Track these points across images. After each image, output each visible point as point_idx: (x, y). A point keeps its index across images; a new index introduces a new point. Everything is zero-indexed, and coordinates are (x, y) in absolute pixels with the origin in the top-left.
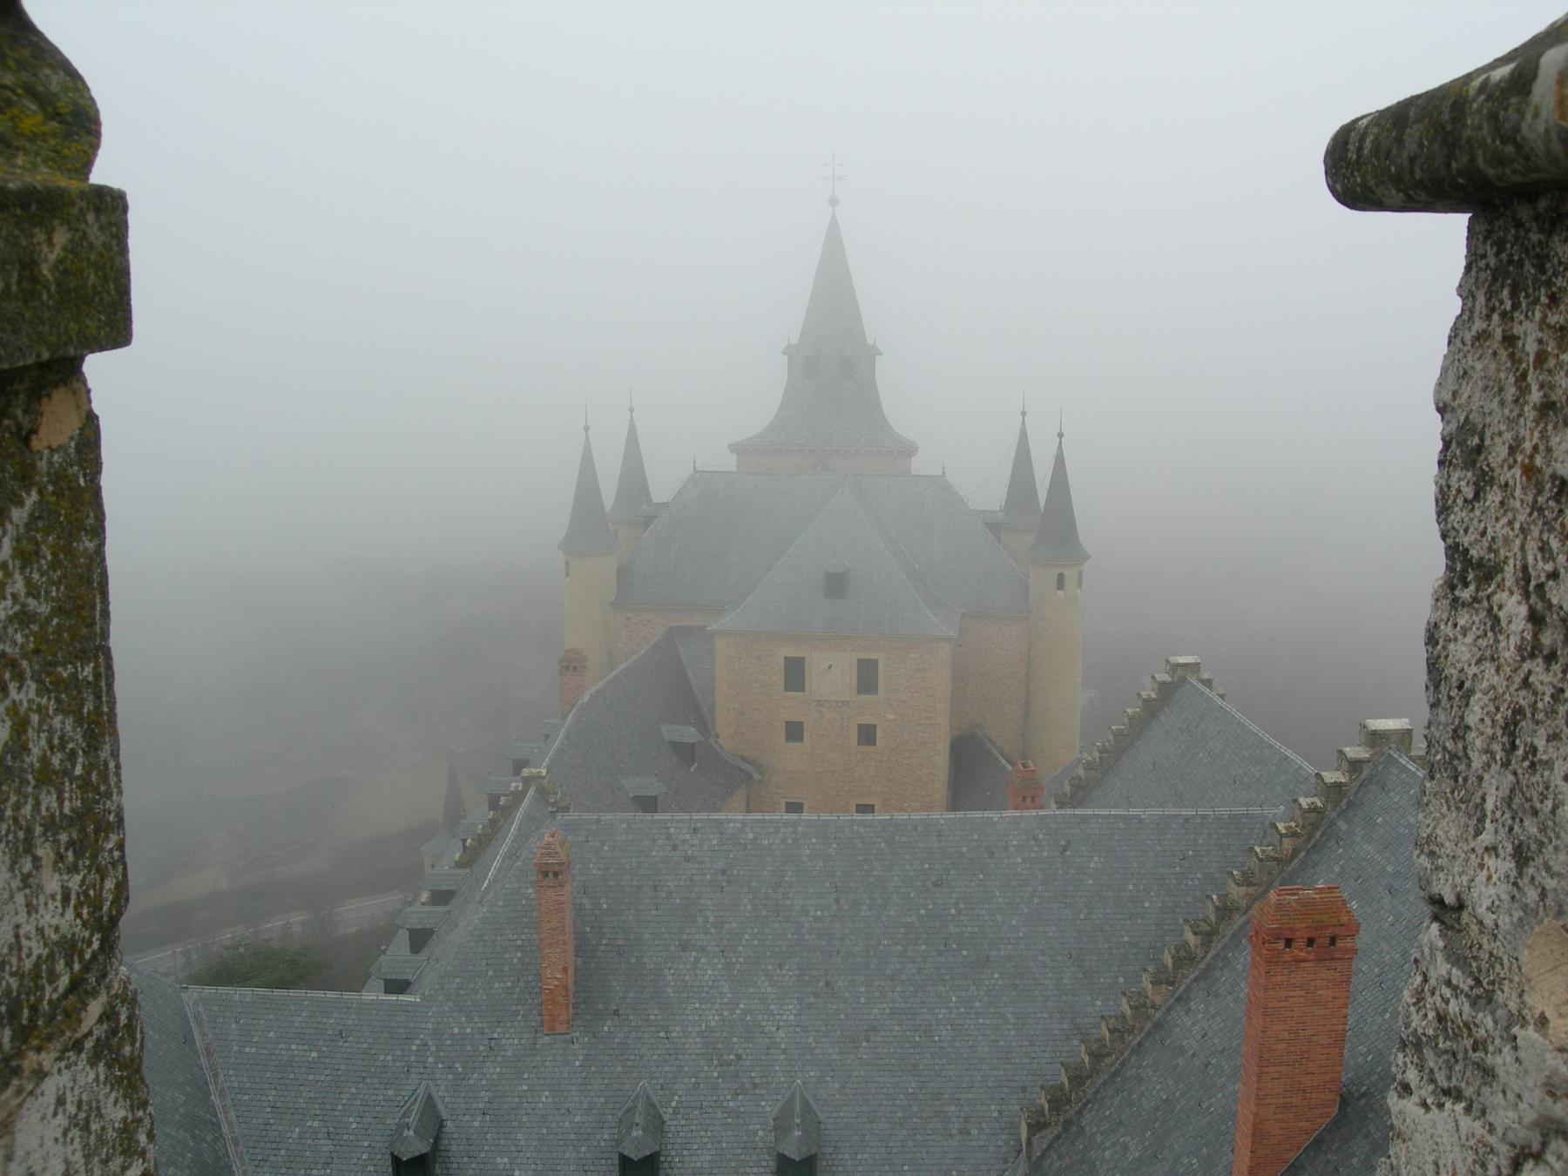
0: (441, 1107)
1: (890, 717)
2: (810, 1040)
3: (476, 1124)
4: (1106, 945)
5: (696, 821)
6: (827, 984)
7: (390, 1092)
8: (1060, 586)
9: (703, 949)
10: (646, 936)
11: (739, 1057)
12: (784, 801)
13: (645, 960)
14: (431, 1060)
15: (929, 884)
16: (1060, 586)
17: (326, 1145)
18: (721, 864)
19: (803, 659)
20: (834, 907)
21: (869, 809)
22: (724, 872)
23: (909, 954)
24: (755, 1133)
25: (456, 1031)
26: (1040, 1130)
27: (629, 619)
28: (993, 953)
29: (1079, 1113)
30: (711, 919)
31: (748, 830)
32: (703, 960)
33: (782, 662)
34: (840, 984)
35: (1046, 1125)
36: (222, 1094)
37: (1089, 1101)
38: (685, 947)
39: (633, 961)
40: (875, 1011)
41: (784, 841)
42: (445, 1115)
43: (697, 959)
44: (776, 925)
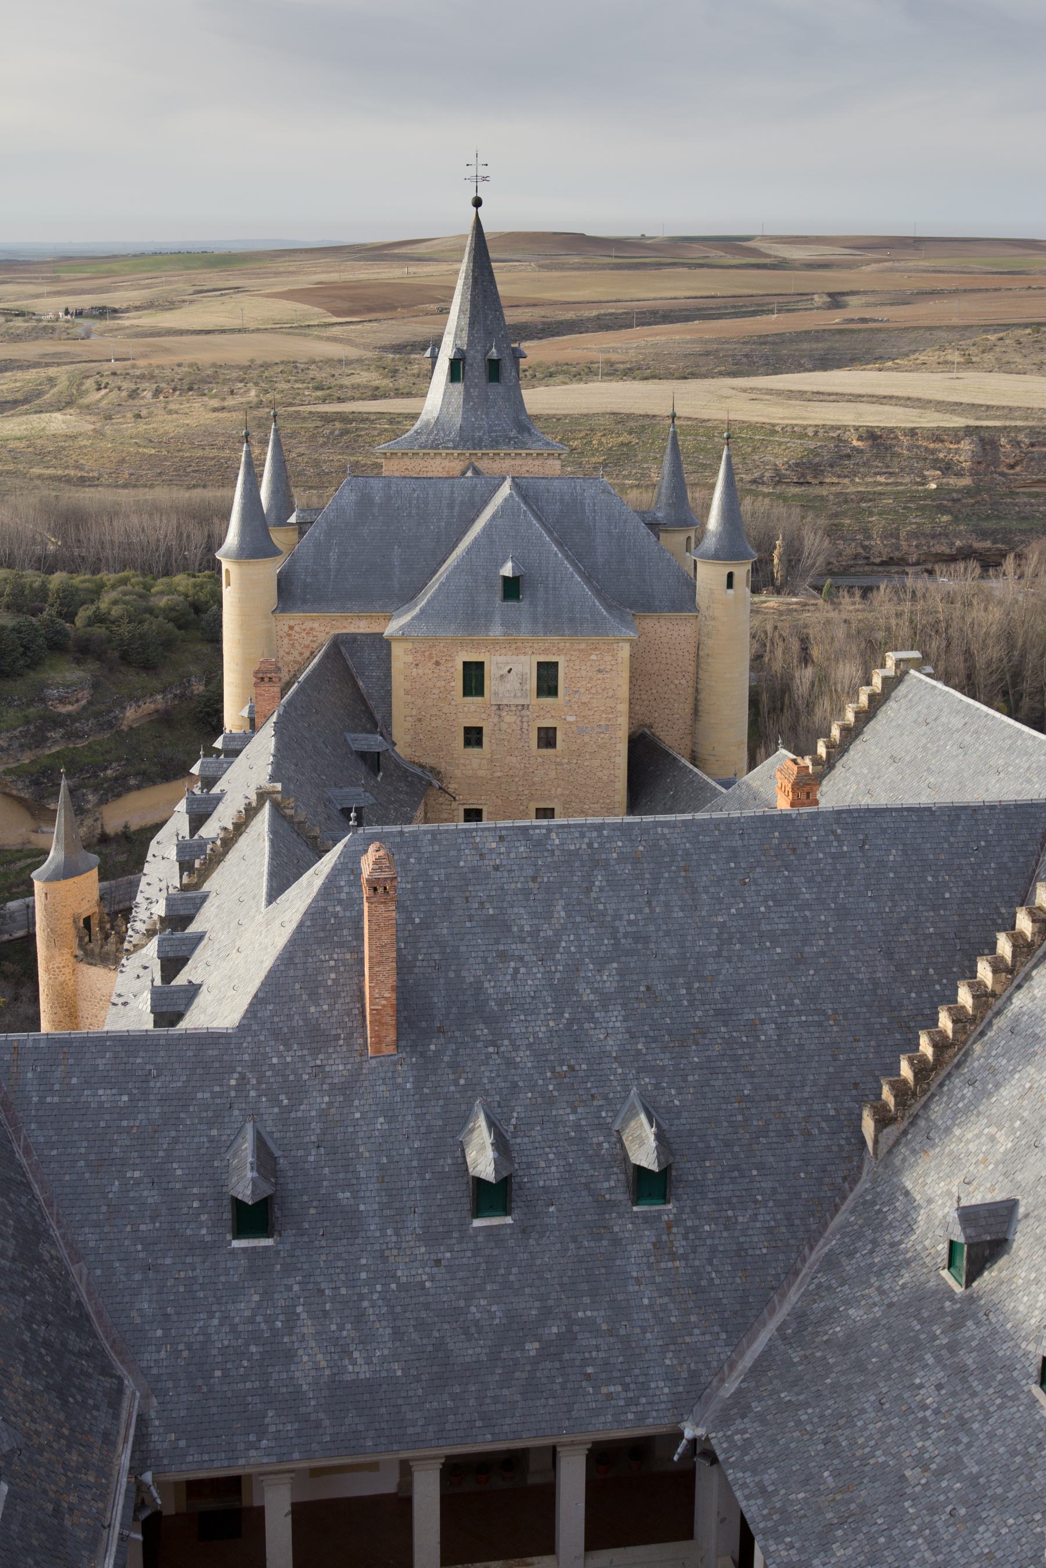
0: (270, 1144)
1: (571, 719)
2: (640, 1046)
3: (312, 1159)
4: (913, 938)
5: (501, 829)
6: (648, 988)
7: (214, 1132)
8: (730, 585)
9: (521, 958)
10: (463, 949)
11: (572, 1068)
12: (462, 808)
13: (464, 973)
14: (253, 1093)
15: (736, 882)
16: (730, 585)
17: (152, 1196)
18: (530, 872)
19: (482, 664)
20: (647, 910)
21: (546, 813)
22: (534, 879)
23: (725, 953)
24: (600, 1144)
25: (275, 1060)
26: (886, 1126)
27: (291, 628)
28: (807, 949)
29: (925, 1106)
30: (527, 928)
31: (553, 835)
32: (522, 970)
33: (460, 667)
34: (660, 987)
35: (892, 1120)
36: (27, 1152)
37: (933, 1095)
38: (503, 956)
39: (452, 975)
40: (699, 1013)
41: (590, 845)
42: (277, 1153)
43: (516, 970)
44: (592, 931)
